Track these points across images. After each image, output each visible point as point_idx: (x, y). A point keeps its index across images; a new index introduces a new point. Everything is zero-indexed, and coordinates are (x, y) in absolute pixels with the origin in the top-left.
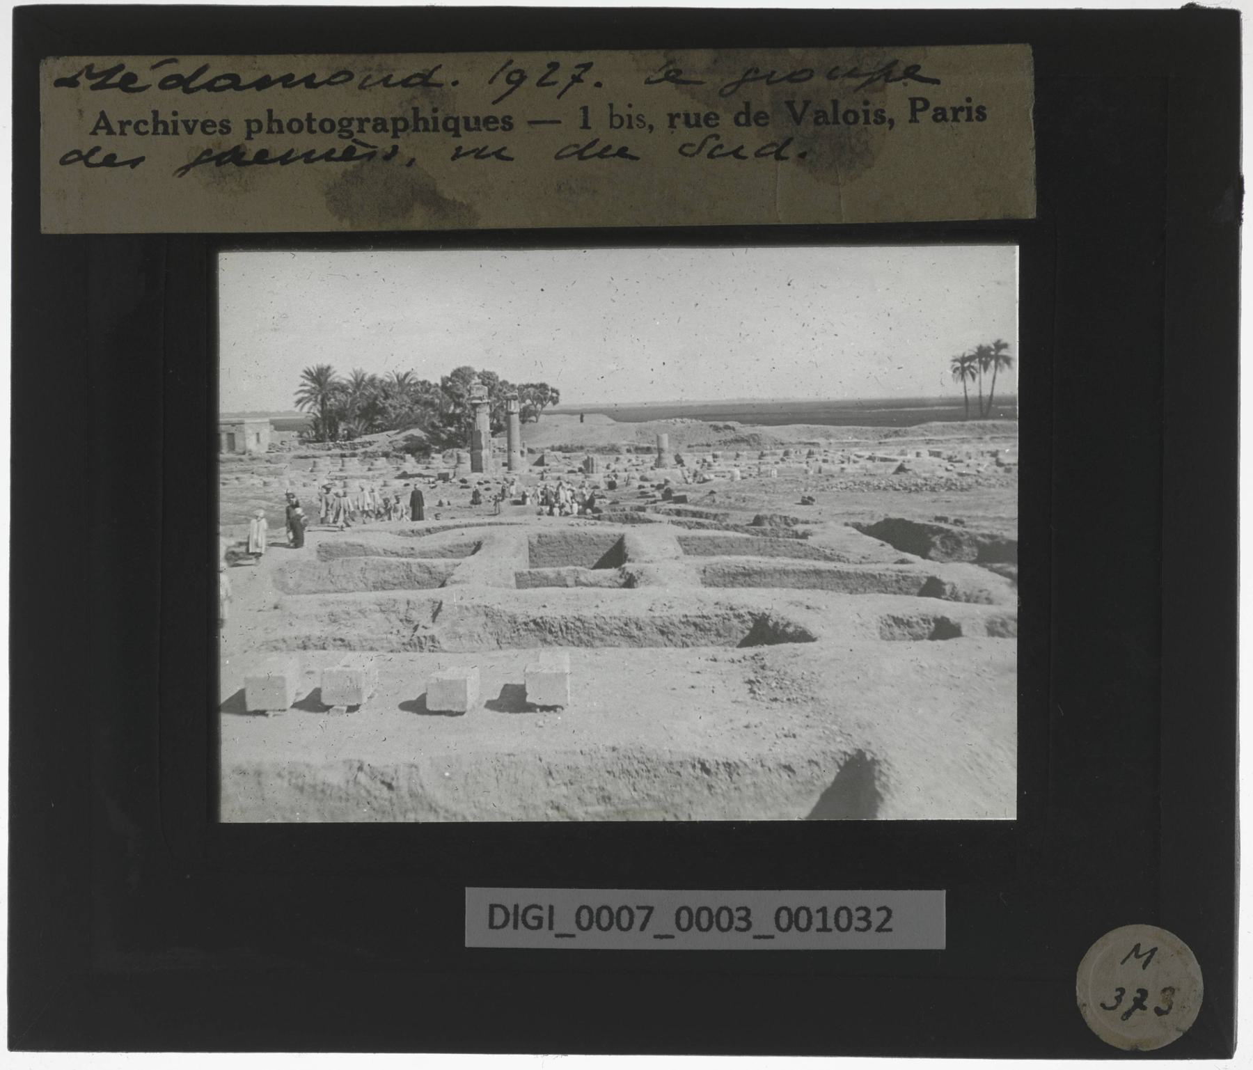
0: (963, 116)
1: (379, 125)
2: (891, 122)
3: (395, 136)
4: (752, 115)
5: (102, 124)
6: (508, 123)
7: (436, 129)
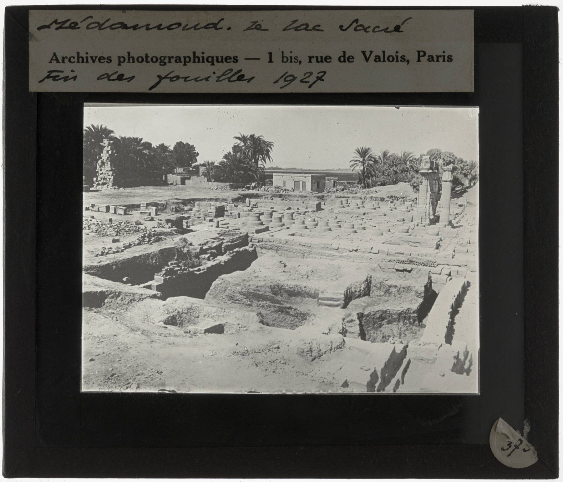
0: (441, 59)
2: (408, 61)
5: (54, 58)
6: (236, 60)
7: (203, 62)
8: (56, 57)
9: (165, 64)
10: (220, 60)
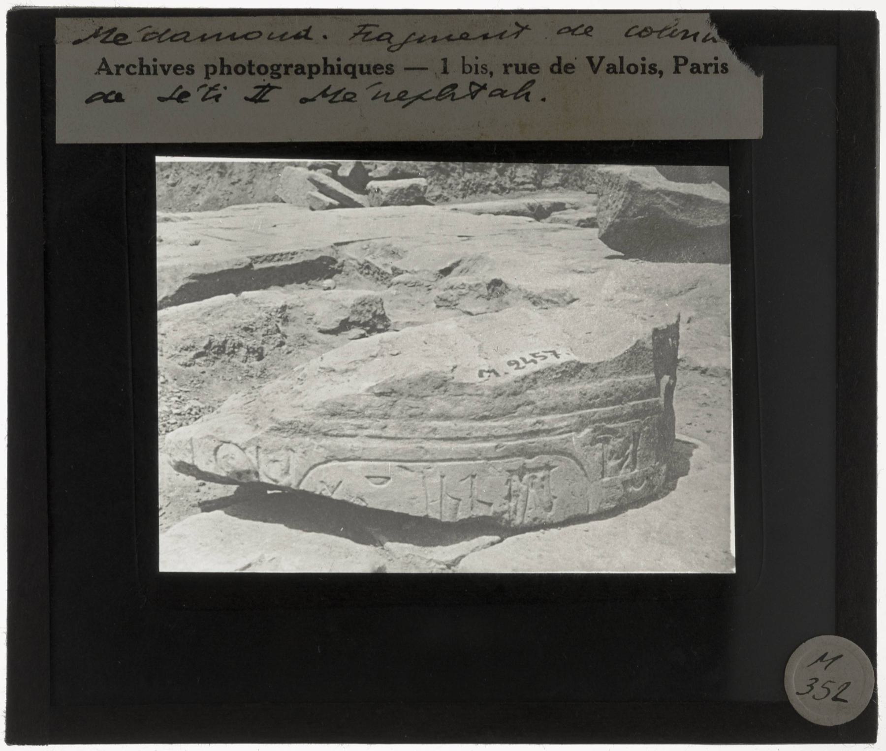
0: (711, 69)
1: (300, 70)
2: (661, 73)
3: (310, 77)
4: (562, 68)
5: (104, 67)
7: (339, 72)
8: (107, 66)
9: (279, 76)
10: (365, 70)
